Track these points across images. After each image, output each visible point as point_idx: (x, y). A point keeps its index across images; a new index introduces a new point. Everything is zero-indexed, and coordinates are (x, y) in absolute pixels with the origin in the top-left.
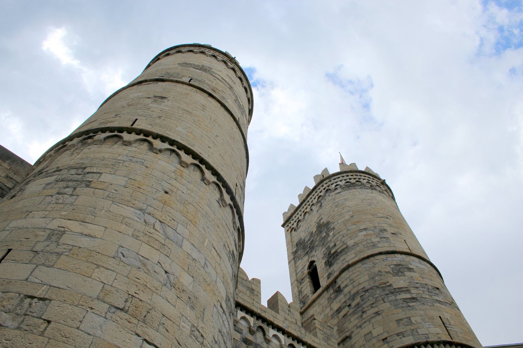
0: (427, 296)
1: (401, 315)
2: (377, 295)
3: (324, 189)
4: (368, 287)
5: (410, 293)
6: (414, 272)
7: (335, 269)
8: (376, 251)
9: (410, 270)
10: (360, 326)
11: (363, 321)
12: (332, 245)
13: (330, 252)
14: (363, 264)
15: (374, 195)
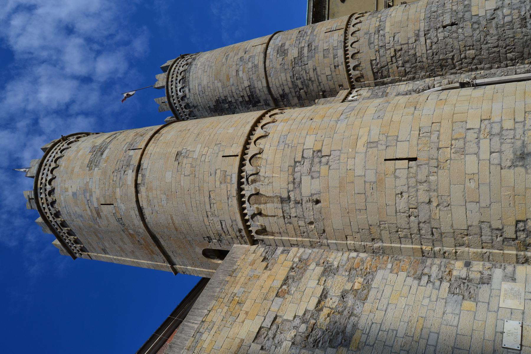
0: (308, 38)
1: (321, 55)
2: (300, 68)
3: (179, 102)
4: (291, 74)
5: (303, 47)
6: (285, 44)
7: (264, 98)
8: (261, 65)
9: (283, 45)
10: (320, 83)
11: (316, 80)
12: (241, 99)
13: (246, 101)
14: (270, 76)
15: (199, 64)
